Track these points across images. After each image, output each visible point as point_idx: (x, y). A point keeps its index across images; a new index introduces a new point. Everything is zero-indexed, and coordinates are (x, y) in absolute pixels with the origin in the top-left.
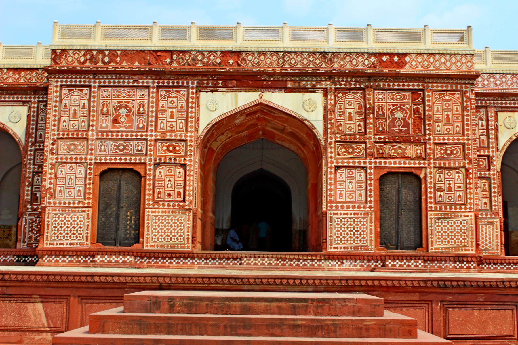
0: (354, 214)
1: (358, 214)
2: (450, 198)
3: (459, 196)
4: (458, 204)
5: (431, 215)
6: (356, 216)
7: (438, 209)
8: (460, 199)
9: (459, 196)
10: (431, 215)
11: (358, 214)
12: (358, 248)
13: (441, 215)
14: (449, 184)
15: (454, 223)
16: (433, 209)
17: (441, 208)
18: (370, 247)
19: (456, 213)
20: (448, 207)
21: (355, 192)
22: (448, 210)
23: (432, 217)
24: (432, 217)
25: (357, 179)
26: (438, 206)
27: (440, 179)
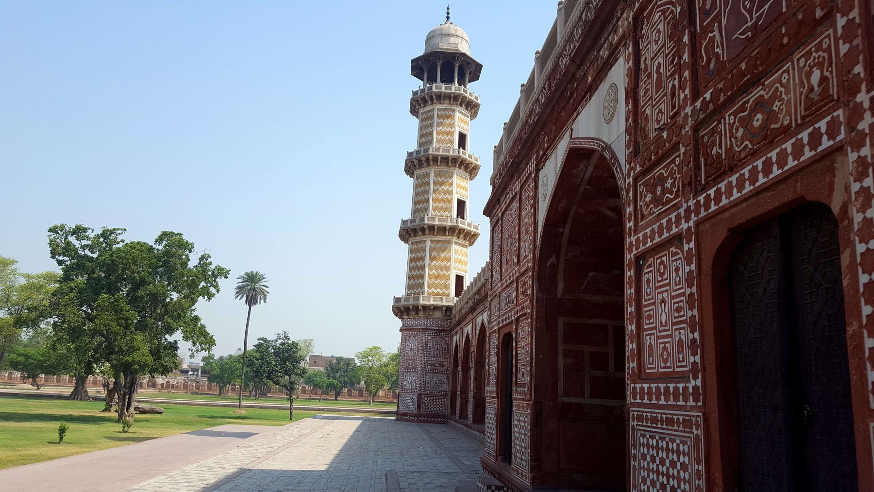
1: (670, 422)
11: (670, 422)
25: (673, 283)
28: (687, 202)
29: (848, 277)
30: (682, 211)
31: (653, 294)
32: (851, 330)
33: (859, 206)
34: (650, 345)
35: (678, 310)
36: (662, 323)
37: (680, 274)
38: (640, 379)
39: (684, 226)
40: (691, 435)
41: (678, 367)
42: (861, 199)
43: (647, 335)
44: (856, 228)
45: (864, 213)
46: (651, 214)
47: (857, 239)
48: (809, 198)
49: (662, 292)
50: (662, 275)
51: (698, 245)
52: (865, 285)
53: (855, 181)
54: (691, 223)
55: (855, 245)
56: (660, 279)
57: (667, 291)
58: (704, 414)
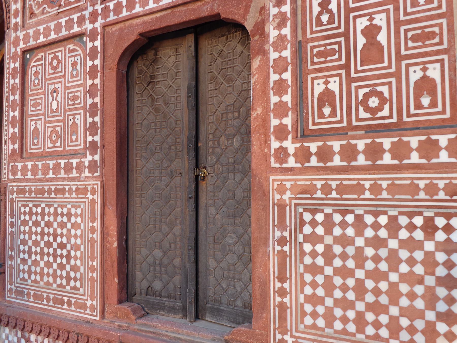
0: (57, 191)
1: (63, 191)
2: (374, 102)
3: (425, 85)
4: (416, 128)
5: (281, 189)
6: (60, 199)
7: (314, 162)
8: (426, 101)
9: (425, 85)
10: (282, 190)
11: (63, 191)
12: (62, 303)
13: (327, 189)
14: (371, 32)
15: (393, 227)
16: (291, 162)
17: (325, 154)
18: (89, 303)
19: (403, 179)
20: (361, 144)
21: (63, 121)
22: (361, 160)
23: (287, 196)
24: (287, 196)
25: (68, 76)
26: (313, 147)
27: (325, 18)
28: (93, 5)
29: (256, 76)
30: (87, 13)
31: (42, 84)
32: (256, 114)
33: (275, 24)
34: (36, 129)
35: (75, 98)
36: (52, 110)
37: (40, 77)
38: (22, 157)
39: (88, 26)
40: (86, 200)
41: (69, 146)
42: (277, 21)
43: (31, 121)
44: (271, 40)
45: (280, 30)
46: (43, 13)
47: (271, 49)
48: (223, 16)
49: (55, 83)
50: (54, 68)
51: (103, 44)
52: (275, 82)
53: (274, 6)
54: (98, 25)
55: (269, 53)
56: (51, 71)
57: (61, 82)
58: (102, 182)
